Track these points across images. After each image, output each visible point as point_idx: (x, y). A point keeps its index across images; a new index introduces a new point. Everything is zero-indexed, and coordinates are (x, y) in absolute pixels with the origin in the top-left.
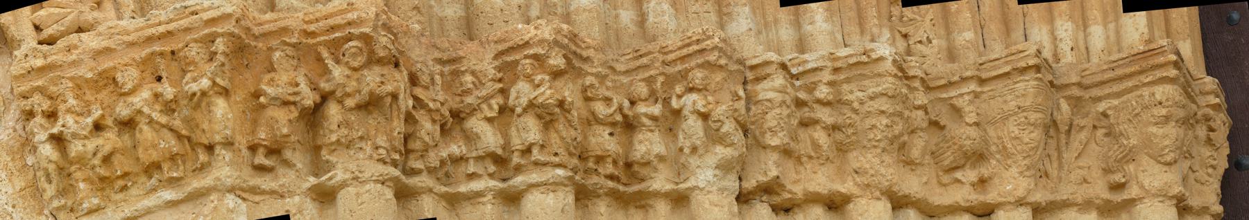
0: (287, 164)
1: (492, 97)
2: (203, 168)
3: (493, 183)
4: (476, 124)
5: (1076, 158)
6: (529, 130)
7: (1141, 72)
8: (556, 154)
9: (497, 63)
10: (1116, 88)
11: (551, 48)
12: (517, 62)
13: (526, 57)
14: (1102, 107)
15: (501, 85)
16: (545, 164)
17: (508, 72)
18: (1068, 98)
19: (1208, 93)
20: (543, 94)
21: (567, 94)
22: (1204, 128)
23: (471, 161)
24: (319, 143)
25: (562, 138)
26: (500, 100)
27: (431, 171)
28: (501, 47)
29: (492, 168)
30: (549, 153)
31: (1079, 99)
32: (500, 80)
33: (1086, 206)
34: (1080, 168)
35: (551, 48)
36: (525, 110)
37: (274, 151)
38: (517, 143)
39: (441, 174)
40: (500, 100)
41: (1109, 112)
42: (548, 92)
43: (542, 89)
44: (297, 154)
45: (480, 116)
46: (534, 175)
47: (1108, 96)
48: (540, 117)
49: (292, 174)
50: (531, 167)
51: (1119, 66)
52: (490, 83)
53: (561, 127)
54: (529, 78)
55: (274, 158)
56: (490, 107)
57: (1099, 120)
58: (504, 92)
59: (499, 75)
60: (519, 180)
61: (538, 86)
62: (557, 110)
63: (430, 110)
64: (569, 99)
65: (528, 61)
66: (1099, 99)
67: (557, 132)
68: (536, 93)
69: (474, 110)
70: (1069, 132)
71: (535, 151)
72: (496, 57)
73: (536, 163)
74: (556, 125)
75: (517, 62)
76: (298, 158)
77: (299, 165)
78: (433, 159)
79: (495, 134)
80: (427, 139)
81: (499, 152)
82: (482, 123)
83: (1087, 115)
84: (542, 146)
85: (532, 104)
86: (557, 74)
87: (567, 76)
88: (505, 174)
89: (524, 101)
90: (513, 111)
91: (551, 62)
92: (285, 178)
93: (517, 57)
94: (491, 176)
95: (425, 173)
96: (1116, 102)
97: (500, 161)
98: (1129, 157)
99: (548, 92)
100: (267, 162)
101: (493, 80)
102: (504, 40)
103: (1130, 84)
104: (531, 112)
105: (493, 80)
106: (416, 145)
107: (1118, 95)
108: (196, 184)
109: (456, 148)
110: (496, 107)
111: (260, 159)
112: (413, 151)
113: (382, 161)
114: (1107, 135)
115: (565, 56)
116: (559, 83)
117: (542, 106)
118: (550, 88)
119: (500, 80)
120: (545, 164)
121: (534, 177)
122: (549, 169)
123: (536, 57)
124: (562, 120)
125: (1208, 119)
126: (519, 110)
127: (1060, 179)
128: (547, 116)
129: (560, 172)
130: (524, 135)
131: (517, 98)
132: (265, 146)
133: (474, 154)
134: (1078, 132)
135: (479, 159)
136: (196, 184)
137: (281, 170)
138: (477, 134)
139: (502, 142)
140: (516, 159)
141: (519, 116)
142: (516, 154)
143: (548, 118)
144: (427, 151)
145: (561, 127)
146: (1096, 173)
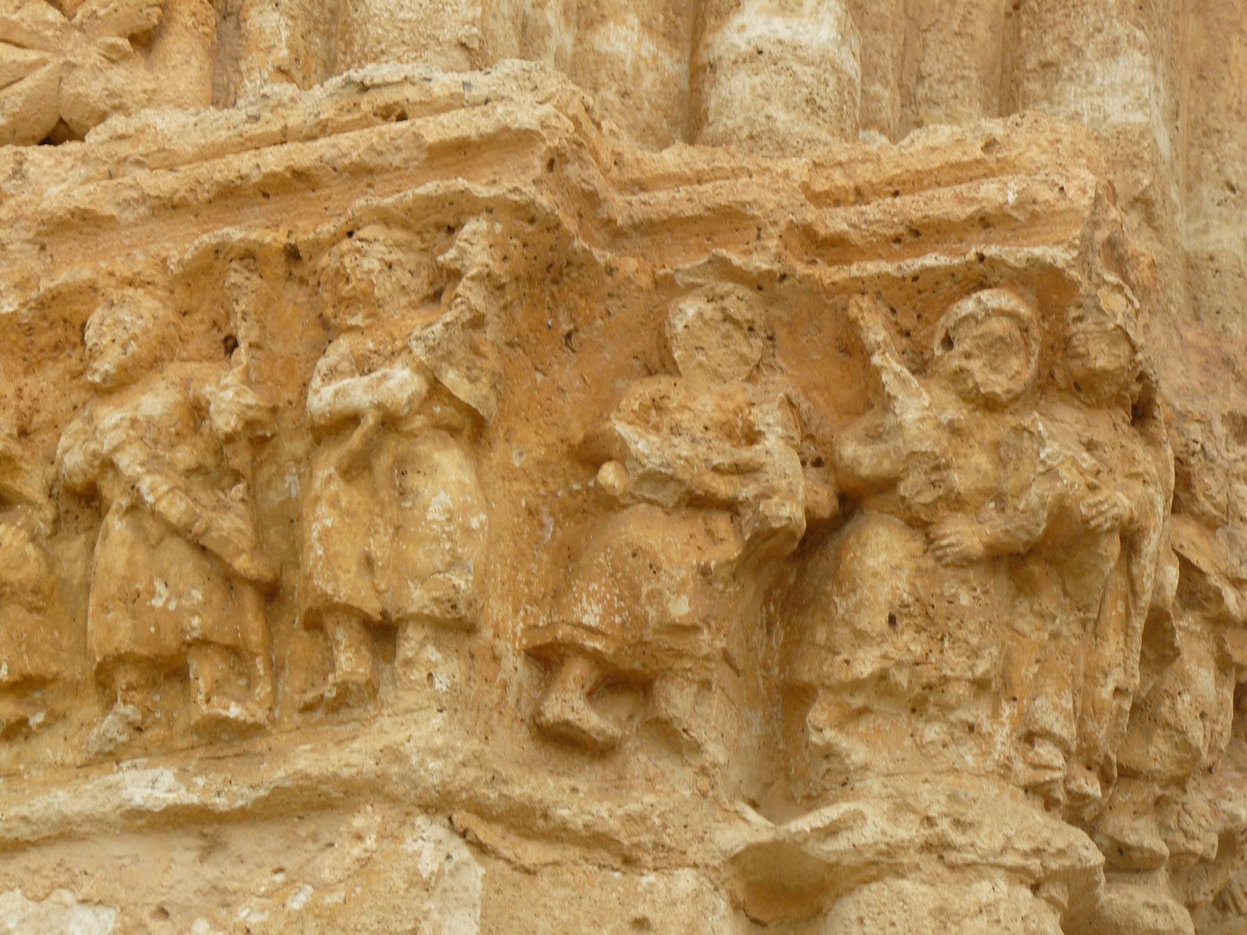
0: (671, 738)
2: (343, 703)
24: (806, 674)
37: (624, 682)
44: (715, 706)
49: (680, 781)
55: (623, 705)
76: (715, 722)
77: (716, 752)
92: (653, 792)
95: (1162, 875)
100: (592, 720)
108: (308, 758)
111: (569, 704)
113: (1040, 793)
132: (596, 658)
136: (308, 758)
137: (641, 760)
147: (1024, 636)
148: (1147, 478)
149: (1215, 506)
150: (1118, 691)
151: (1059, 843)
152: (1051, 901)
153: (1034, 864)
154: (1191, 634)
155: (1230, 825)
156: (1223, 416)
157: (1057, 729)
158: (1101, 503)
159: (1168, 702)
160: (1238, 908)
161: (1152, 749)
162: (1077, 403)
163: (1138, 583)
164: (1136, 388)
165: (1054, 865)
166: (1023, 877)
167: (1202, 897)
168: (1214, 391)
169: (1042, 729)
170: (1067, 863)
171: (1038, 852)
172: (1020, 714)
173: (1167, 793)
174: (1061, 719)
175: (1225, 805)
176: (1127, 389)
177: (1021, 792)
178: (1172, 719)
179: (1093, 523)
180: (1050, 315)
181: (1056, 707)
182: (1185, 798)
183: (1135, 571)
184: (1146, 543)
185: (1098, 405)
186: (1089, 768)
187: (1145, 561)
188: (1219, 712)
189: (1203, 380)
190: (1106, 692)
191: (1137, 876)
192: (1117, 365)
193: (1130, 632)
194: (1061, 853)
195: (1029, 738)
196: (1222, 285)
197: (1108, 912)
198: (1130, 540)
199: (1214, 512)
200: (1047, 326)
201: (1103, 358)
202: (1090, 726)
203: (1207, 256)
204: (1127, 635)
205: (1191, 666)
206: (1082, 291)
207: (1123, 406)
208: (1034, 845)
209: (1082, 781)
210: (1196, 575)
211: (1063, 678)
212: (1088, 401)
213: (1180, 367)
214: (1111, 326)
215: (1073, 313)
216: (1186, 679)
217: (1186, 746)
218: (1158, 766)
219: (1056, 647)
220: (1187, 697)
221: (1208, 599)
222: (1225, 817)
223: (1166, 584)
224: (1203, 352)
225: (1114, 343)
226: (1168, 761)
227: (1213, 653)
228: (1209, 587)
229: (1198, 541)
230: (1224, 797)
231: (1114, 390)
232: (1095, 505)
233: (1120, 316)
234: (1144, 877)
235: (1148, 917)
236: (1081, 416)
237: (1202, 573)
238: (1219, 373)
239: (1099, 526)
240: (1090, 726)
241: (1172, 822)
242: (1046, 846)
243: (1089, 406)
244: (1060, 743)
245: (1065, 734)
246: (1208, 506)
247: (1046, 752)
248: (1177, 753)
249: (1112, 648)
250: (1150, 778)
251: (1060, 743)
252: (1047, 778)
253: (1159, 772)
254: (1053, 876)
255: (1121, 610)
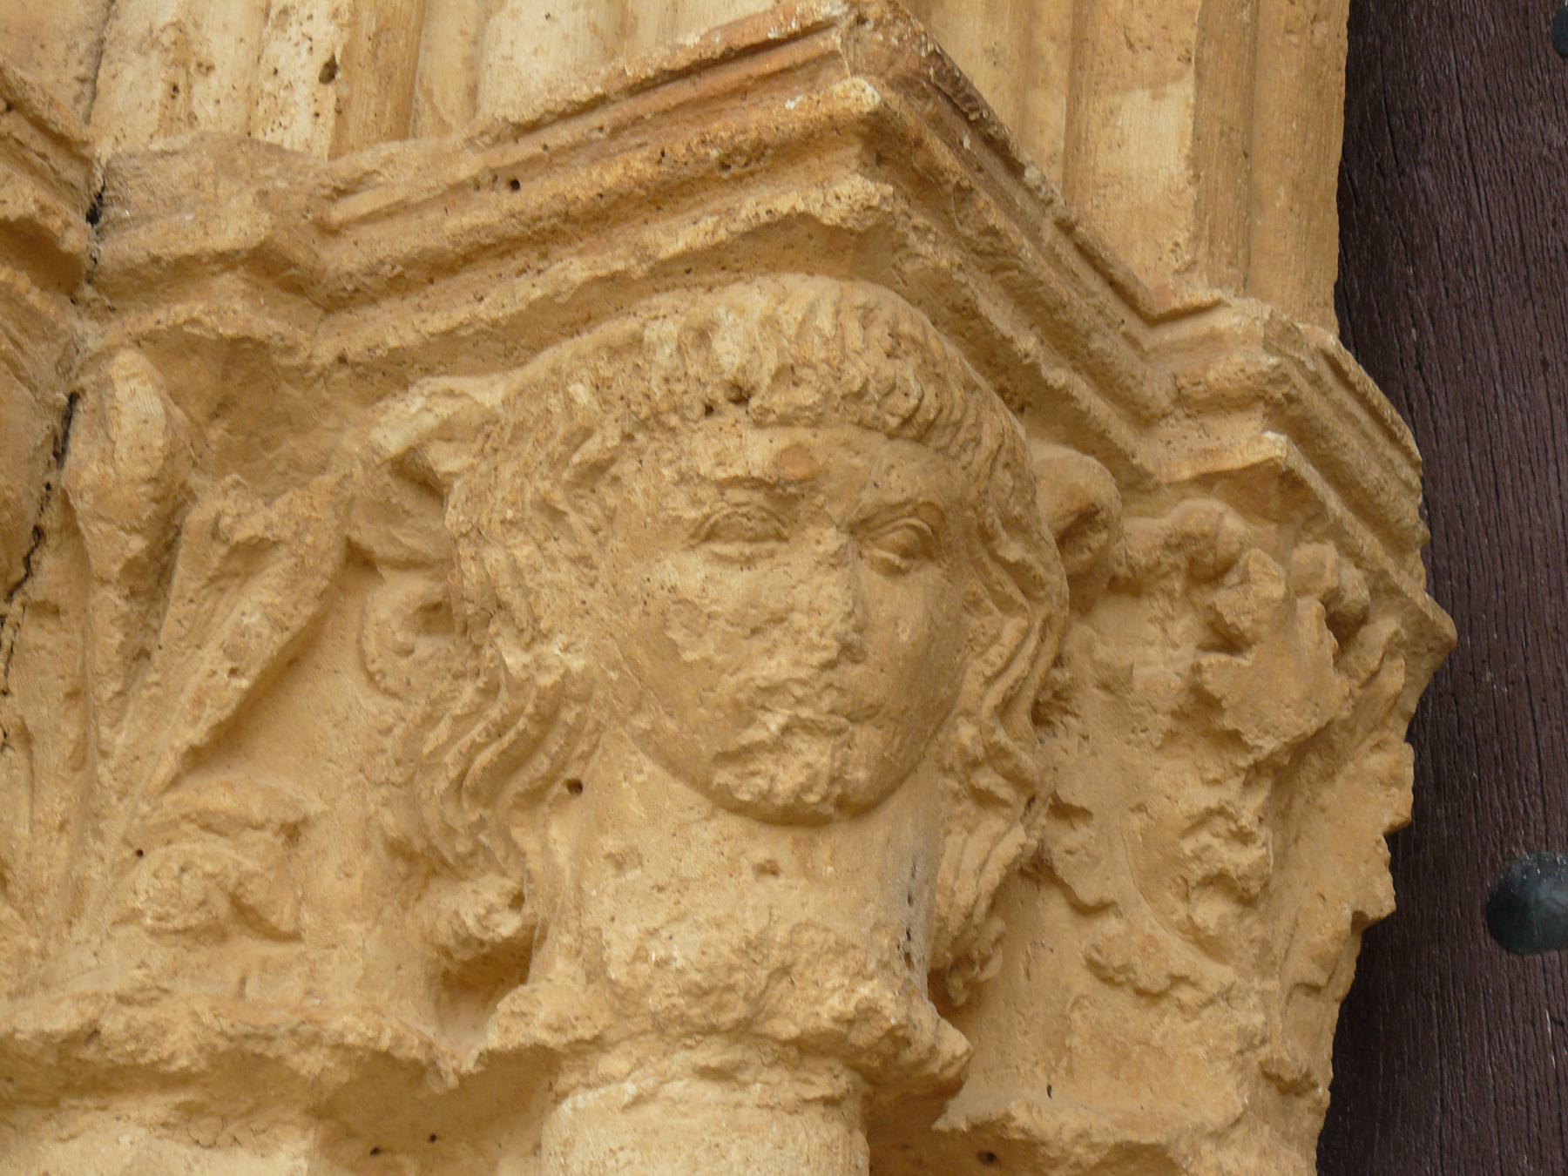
5: (198, 759)
7: (665, 195)
10: (507, 295)
14: (399, 423)
18: (170, 349)
19: (1225, 403)
22: (1185, 626)
31: (242, 355)
33: (234, 1084)
34: (208, 824)
41: (446, 460)
47: (449, 352)
51: (547, 162)
57: (388, 512)
66: (388, 374)
70: (151, 578)
83: (300, 473)
96: (488, 392)
98: (535, 762)
103: (574, 268)
107: (509, 343)
114: (434, 615)
125: (1208, 569)
127: (78, 890)
134: (218, 581)
146: (339, 871)
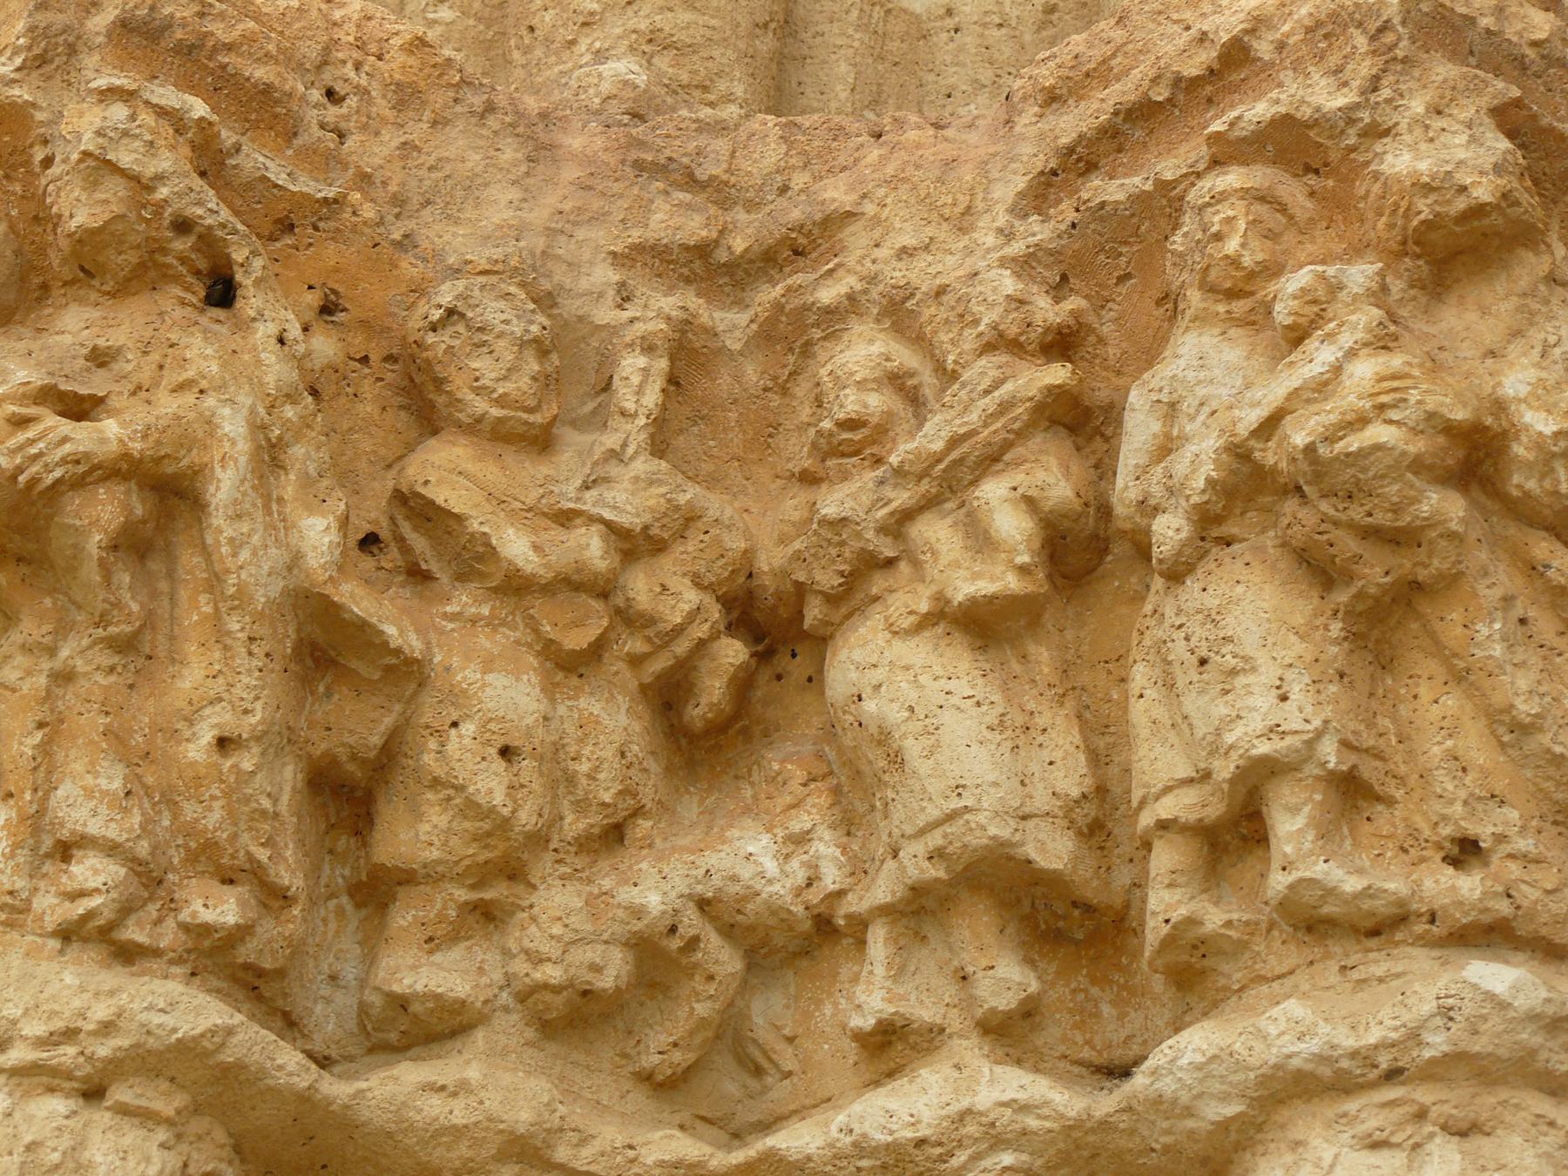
1: (992, 460)
3: (1000, 1086)
4: (888, 670)
6: (1243, 666)
8: (1465, 852)
9: (1039, 231)
11: (1391, 63)
12: (1165, 203)
13: (1225, 153)
15: (1058, 374)
16: (1381, 927)
17: (1107, 275)
20: (1324, 386)
21: (1516, 381)
23: (878, 942)
25: (1513, 730)
26: (1052, 476)
27: (571, 1019)
28: (1071, 124)
29: (1006, 978)
30: (1408, 847)
32: (1062, 344)
35: (1391, 63)
36: (1211, 528)
38: (1168, 778)
39: (662, 1041)
40: (1052, 476)
42: (1364, 370)
43: (1319, 356)
45: (907, 599)
46: (1294, 1008)
48: (1317, 568)
50: (1278, 954)
52: (984, 369)
53: (1489, 638)
54: (1240, 292)
56: (981, 540)
58: (1082, 422)
59: (1048, 311)
60: (1191, 1058)
61: (1297, 336)
62: (1444, 505)
63: (516, 586)
64: (1541, 423)
65: (1232, 178)
67: (1460, 676)
68: (1274, 391)
69: (864, 573)
71: (1291, 823)
72: (1043, 191)
73: (1316, 924)
74: (1451, 624)
75: (1165, 203)
78: (566, 927)
79: (1018, 732)
80: (491, 784)
81: (1052, 850)
82: (917, 651)
84: (1352, 793)
85: (1248, 485)
86: (1450, 252)
87: (1530, 267)
88: (1112, 1031)
89: (1200, 461)
90: (1143, 550)
91: (1401, 161)
93: (1170, 168)
94: (1009, 1033)
97: (1069, 923)
99: (1364, 370)
101: (997, 343)
102: (1101, 74)
104: (1260, 542)
105: (997, 343)
106: (416, 833)
109: (761, 853)
110: (1014, 528)
112: (407, 878)
115: (1508, 118)
116: (1470, 318)
117: (1319, 474)
118: (1383, 342)
119: (1062, 344)
120: (1381, 927)
121: (1294, 1020)
122: (1418, 960)
123: (1293, 144)
124: (1496, 580)
126: (1170, 531)
128: (1376, 558)
129: (1496, 976)
130: (1205, 708)
131: (1165, 448)
133: (883, 889)
135: (919, 910)
138: (883, 738)
139: (1071, 778)
140: (1168, 899)
141: (1176, 575)
142: (1165, 858)
143: (1376, 571)
144: (513, 872)
145: (1489, 638)
147: (14, 690)
148: (204, 384)
149: (501, 401)
150: (223, 743)
151: (101, 1011)
152: (123, 1110)
153: (67, 1054)
154: (474, 621)
155: (638, 926)
156: (614, 254)
157: (94, 828)
158: (31, 442)
159: (433, 744)
160: (776, 1065)
161: (425, 827)
162: (94, 296)
163: (215, 557)
164: (182, 245)
165: (103, 1050)
166: (45, 1079)
167: (656, 1059)
168: (598, 218)
169: (73, 832)
170: (125, 1042)
171: (70, 1034)
172: (23, 819)
173: (488, 895)
174: (103, 810)
175: (627, 895)
176: (164, 251)
177: (54, 944)
178: (440, 772)
179: (22, 479)
180: (14, 167)
181: (89, 793)
182: (533, 899)
183: (209, 540)
184: (212, 489)
185: (123, 290)
186: (231, 882)
187: (218, 519)
188: (581, 741)
189: (567, 206)
190: (198, 749)
191: (449, 1045)
192: (107, 216)
193: (229, 642)
194: (107, 1028)
195: (65, 851)
196: (961, 49)
197: (365, 1114)
198: (167, 493)
199: (496, 412)
200: (18, 188)
201: (80, 209)
202: (190, 810)
203: (942, 11)
204: (226, 648)
205: (467, 675)
206: (40, 116)
207: (176, 279)
208: (59, 1024)
209: (197, 905)
210: (452, 522)
211: (92, 742)
212: (106, 288)
213: (514, 194)
214: (75, 156)
215: (39, 154)
216: (457, 696)
217: (472, 808)
218: (435, 854)
219: (77, 696)
220: (468, 728)
221: (480, 558)
222: (620, 913)
223: (306, 547)
224: (587, 160)
225: (92, 184)
226: (454, 841)
227: (530, 645)
228: (472, 535)
229: (470, 467)
230: (626, 882)
231: (132, 257)
232: (21, 448)
233: (88, 136)
234: (458, 1044)
235: (435, 1106)
236: (96, 314)
237: (459, 518)
238: (617, 187)
239: (33, 482)
240: (190, 810)
241: (513, 945)
242: (79, 1024)
243: (112, 295)
244: (112, 849)
245: (112, 833)
246: (480, 405)
247: (91, 871)
248: (467, 825)
249: (192, 677)
250: (431, 876)
251: (112, 849)
252: (81, 911)
253: (438, 862)
254: (116, 1068)
255: (208, 609)
